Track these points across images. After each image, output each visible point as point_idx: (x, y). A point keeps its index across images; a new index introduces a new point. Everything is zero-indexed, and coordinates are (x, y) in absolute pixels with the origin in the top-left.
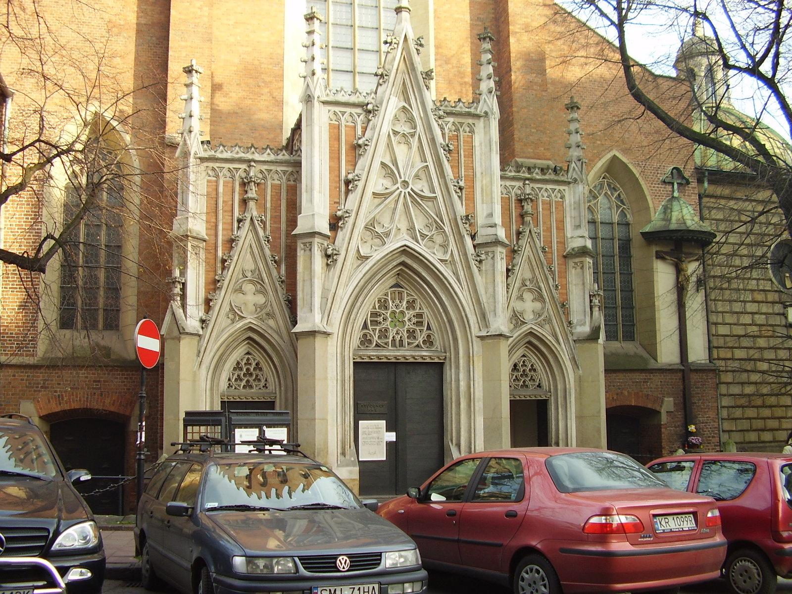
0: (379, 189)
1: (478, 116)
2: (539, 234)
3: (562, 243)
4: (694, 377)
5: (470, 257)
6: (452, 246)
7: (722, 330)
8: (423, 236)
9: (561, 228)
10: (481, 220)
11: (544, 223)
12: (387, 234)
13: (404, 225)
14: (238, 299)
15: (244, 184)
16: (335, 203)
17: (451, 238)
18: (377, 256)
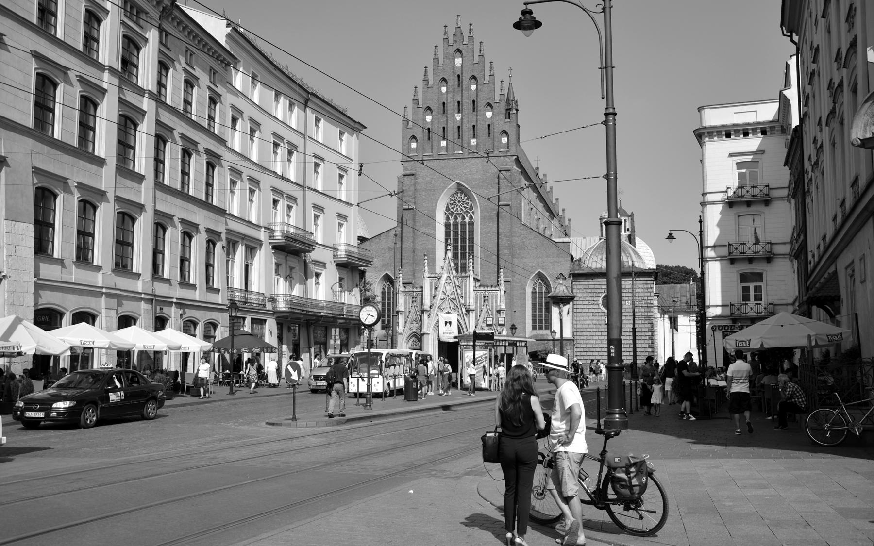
0: (442, 298)
1: (467, 277)
3: (496, 307)
4: (565, 342)
7: (578, 326)
10: (467, 304)
13: (448, 306)
14: (412, 326)
15: (413, 298)
16: (431, 302)
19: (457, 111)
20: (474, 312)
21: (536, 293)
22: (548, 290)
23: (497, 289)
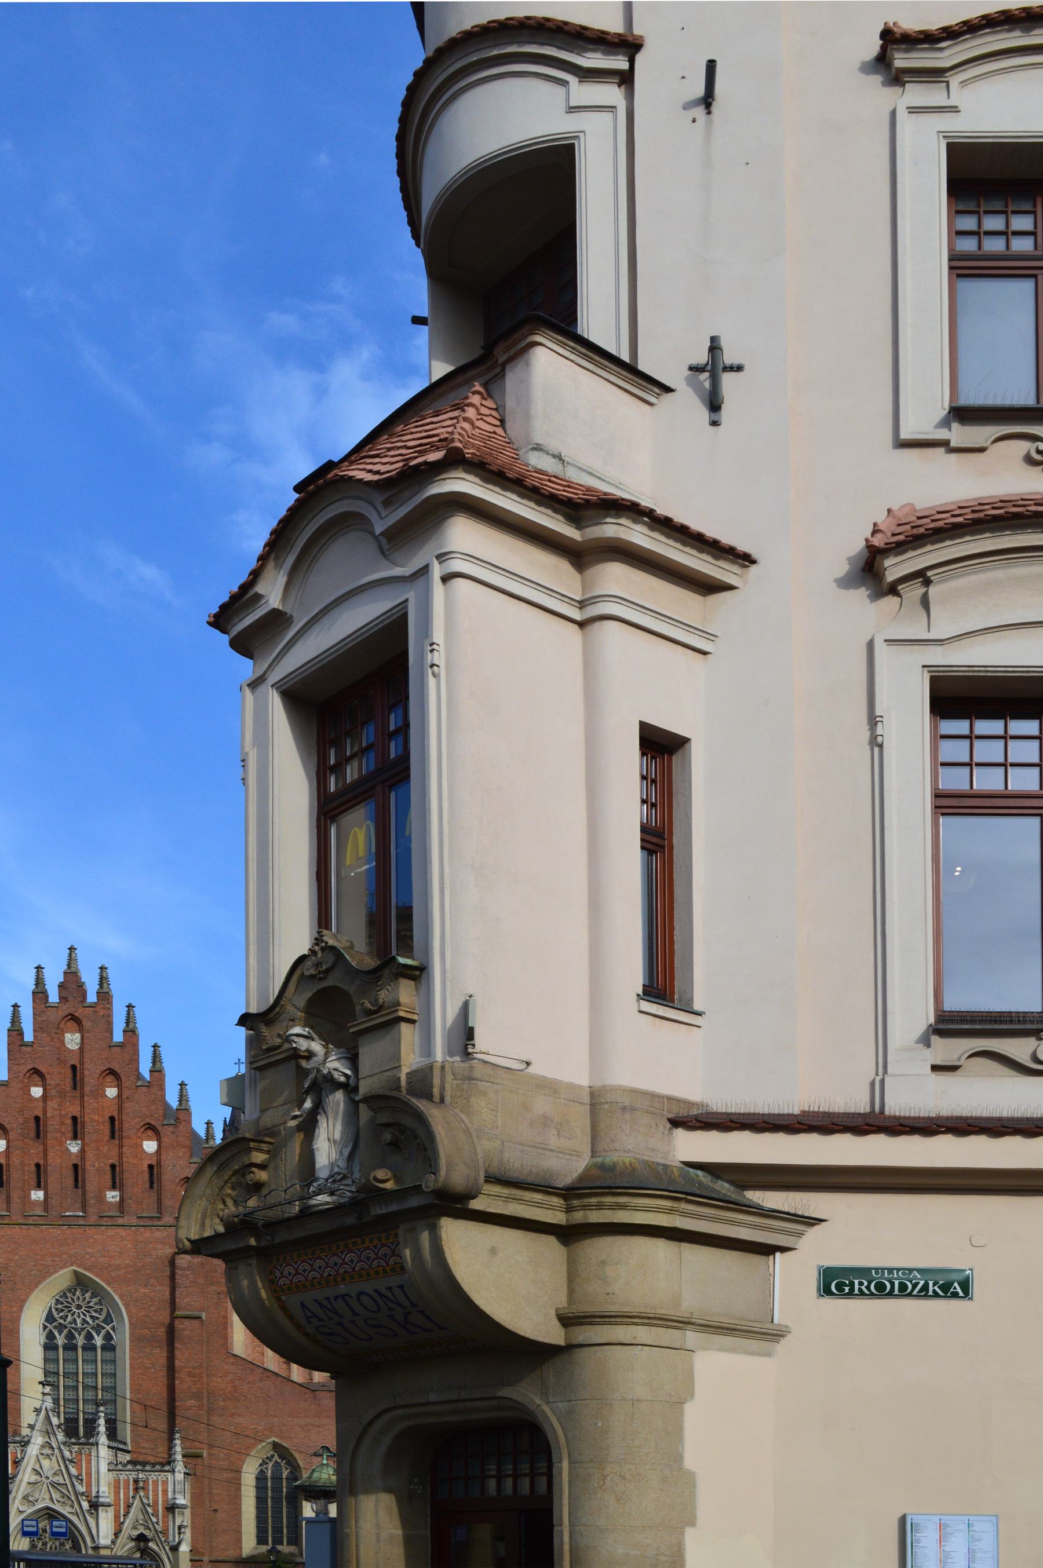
2: (148, 1498)
5: (85, 1511)
6: (76, 1506)
8: (58, 1501)
9: (165, 1492)
11: (153, 1491)
12: (37, 1501)
13: (47, 1497)
17: (75, 1503)
18: (29, 1511)
19: (70, 1135)
20: (111, 1510)
21: (266, 1478)
22: (294, 1476)
23: (167, 1468)
